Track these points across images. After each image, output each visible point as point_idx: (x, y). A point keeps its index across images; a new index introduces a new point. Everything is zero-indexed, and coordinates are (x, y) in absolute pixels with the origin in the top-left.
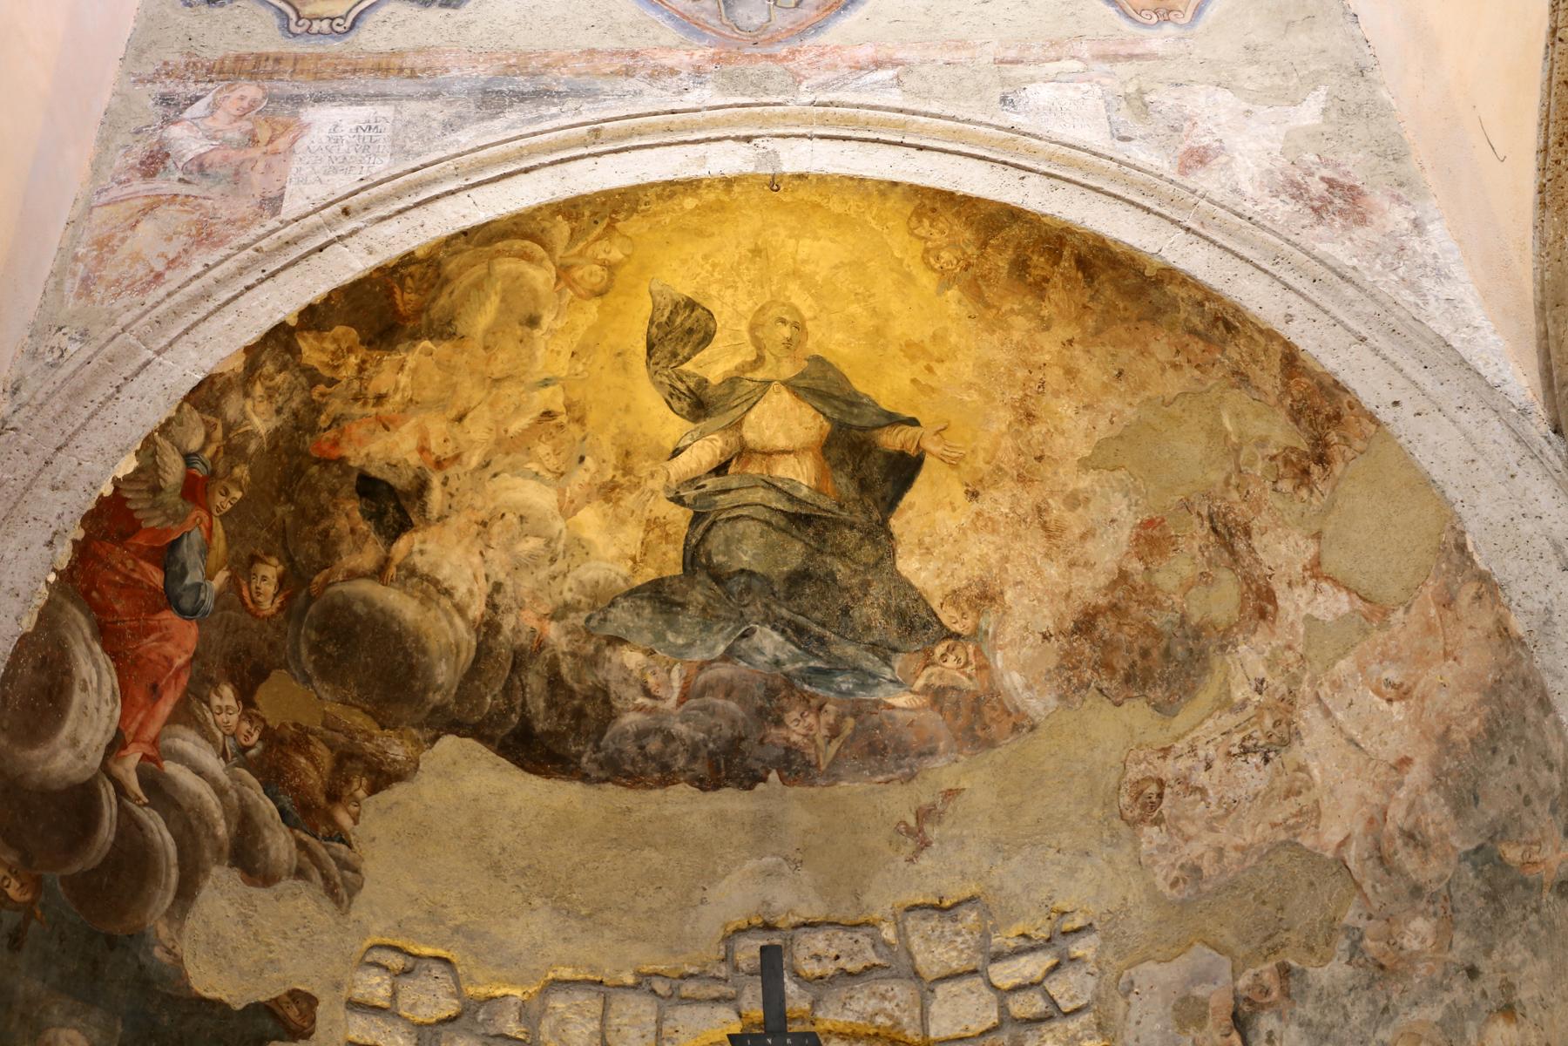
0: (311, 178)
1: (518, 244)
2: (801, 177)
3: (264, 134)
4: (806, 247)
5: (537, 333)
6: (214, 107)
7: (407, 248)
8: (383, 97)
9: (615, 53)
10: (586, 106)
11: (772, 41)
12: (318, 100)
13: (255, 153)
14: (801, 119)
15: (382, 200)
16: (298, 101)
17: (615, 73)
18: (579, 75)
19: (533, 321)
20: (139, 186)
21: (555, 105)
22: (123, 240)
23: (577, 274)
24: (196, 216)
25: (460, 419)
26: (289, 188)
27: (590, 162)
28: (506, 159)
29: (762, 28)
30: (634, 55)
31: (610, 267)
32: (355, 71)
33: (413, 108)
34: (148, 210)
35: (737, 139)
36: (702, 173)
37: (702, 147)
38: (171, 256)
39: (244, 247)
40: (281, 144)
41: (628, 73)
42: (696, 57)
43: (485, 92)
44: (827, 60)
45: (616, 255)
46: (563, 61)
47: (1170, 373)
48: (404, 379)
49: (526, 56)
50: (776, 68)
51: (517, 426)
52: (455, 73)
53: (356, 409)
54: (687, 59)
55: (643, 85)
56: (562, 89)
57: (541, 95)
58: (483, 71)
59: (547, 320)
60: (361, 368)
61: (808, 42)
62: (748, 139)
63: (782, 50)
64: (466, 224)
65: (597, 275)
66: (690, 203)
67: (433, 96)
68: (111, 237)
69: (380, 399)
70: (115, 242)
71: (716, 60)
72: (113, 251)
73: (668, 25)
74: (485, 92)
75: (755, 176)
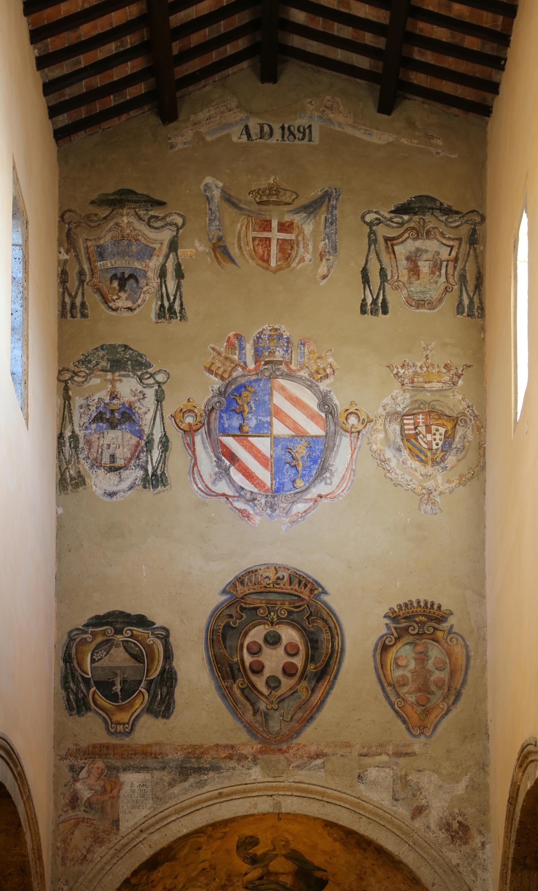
0: (127, 811)
1: (195, 835)
2: (288, 813)
3: (108, 788)
4: (289, 826)
5: (201, 851)
6: (89, 772)
7: (162, 846)
8: (146, 769)
9: (226, 746)
10: (216, 775)
11: (281, 742)
12: (124, 770)
13: (106, 797)
14: (289, 788)
15: (152, 825)
16: (117, 769)
17: (226, 758)
18: (213, 758)
19: (200, 849)
20: (71, 813)
21: (206, 774)
22: (71, 839)
23: (214, 836)
24: (92, 829)
25: (176, 877)
26: (121, 815)
27: (218, 805)
28: (191, 806)
29: (278, 733)
30: (232, 747)
31: (225, 833)
32: (135, 754)
33: (157, 774)
34: (76, 825)
35: (267, 795)
36: (256, 812)
37: (256, 799)
38: (88, 847)
39: (111, 848)
40: (115, 792)
41: (230, 757)
42: (254, 749)
43: (182, 768)
44: (300, 753)
45: (227, 830)
46: (206, 751)
47: (402, 884)
48: (159, 874)
49: (194, 747)
50: (282, 757)
51: (193, 874)
52: (170, 756)
53: (146, 887)
54: (251, 750)
55: (236, 765)
56: (208, 766)
57: (200, 770)
58: (180, 755)
59: (204, 847)
60: (147, 877)
61: (295, 741)
62: (271, 796)
63: (284, 747)
64: (180, 835)
65: (221, 835)
66: (251, 819)
67: (163, 768)
68: (67, 838)
69: (152, 882)
70: (68, 841)
71: (261, 752)
72: (69, 845)
73: (244, 730)
74: (182, 768)
75: (273, 813)
